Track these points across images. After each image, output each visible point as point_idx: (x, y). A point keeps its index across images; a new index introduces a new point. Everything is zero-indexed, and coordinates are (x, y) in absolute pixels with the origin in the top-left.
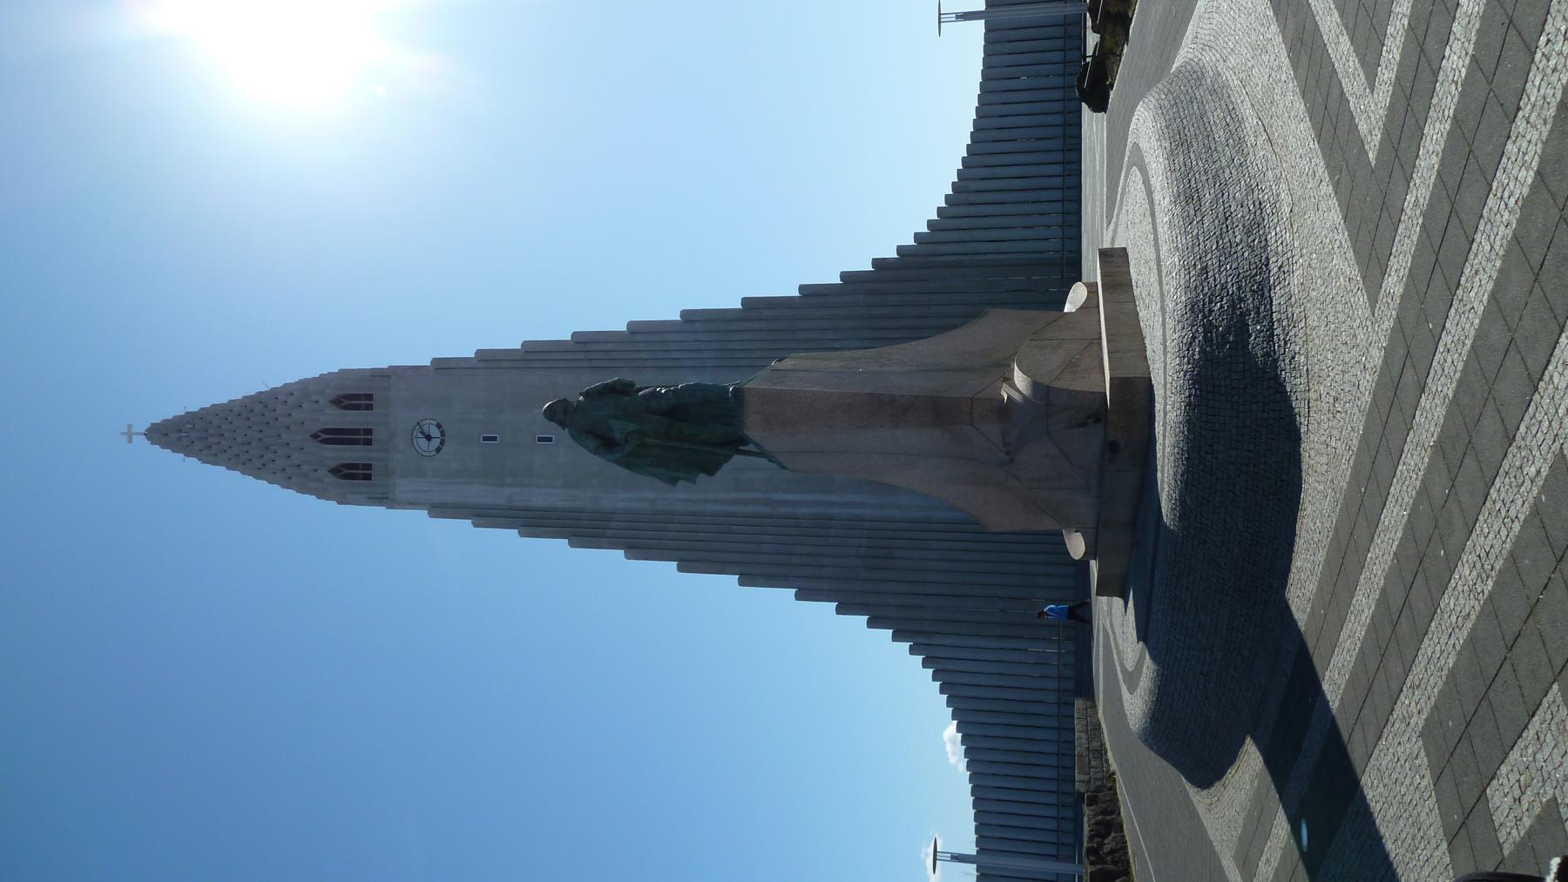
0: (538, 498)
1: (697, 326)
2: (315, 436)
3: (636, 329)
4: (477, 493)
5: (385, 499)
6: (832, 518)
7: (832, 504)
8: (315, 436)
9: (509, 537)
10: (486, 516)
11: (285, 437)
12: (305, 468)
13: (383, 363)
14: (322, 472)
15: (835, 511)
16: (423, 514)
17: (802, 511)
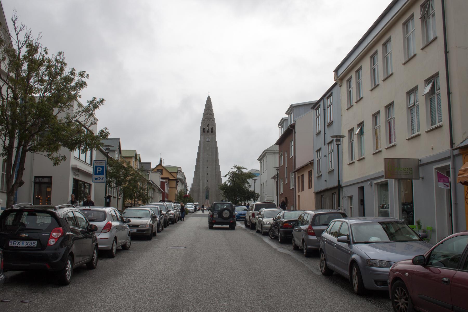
0: (201, 153)
1: (219, 173)
2: (208, 124)
3: (219, 166)
4: (202, 146)
5: (201, 134)
6: (200, 186)
7: (201, 186)
8: (208, 124)
9: (197, 150)
10: (199, 148)
11: (208, 120)
12: (205, 123)
13: (217, 134)
14: (204, 126)
15: (200, 187)
16: (200, 140)
17: (200, 183)
